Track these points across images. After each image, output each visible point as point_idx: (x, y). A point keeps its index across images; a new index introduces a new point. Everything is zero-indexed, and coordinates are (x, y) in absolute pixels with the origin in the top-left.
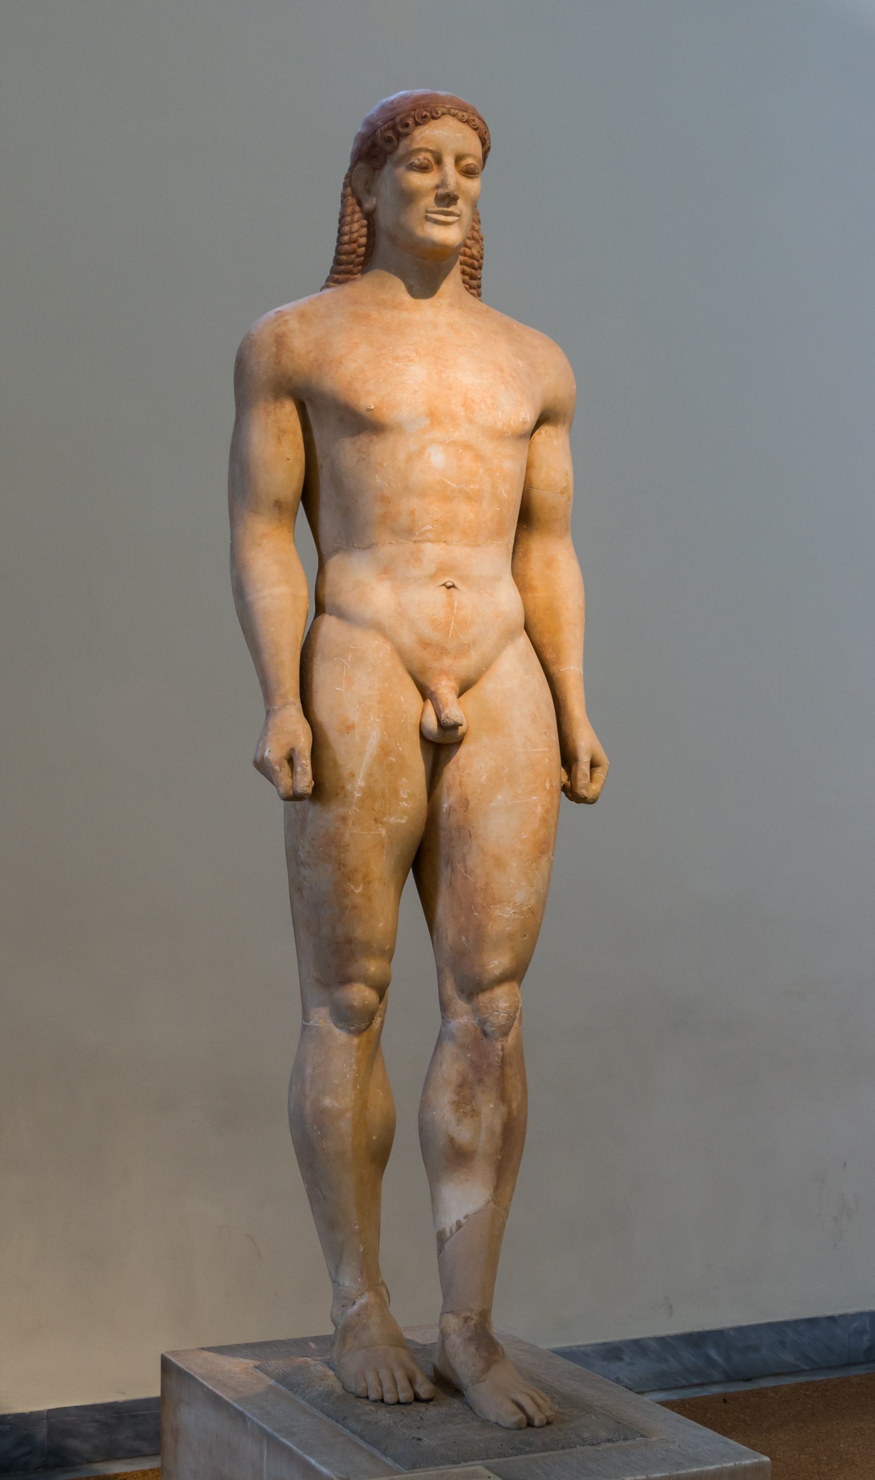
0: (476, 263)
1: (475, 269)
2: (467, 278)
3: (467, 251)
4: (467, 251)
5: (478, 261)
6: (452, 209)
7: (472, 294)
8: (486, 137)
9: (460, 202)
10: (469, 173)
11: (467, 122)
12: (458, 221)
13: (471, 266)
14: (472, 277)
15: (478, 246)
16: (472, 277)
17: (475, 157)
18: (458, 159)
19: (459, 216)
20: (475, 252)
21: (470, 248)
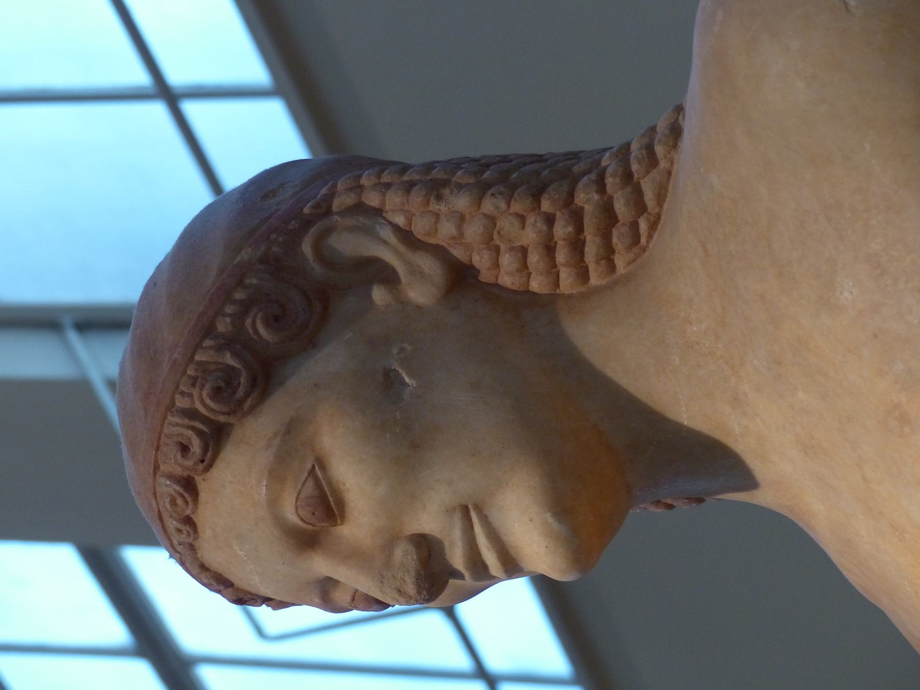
0: (562, 230)
1: (577, 217)
2: (618, 239)
3: (534, 258)
4: (534, 258)
5: (550, 220)
6: (457, 558)
7: (661, 198)
8: (196, 446)
9: (429, 519)
10: (328, 506)
11: (189, 521)
12: (479, 509)
13: (577, 245)
14: (609, 216)
15: (507, 224)
16: (609, 216)
17: (273, 503)
18: (306, 540)
19: (465, 510)
20: (530, 236)
21: (524, 251)
